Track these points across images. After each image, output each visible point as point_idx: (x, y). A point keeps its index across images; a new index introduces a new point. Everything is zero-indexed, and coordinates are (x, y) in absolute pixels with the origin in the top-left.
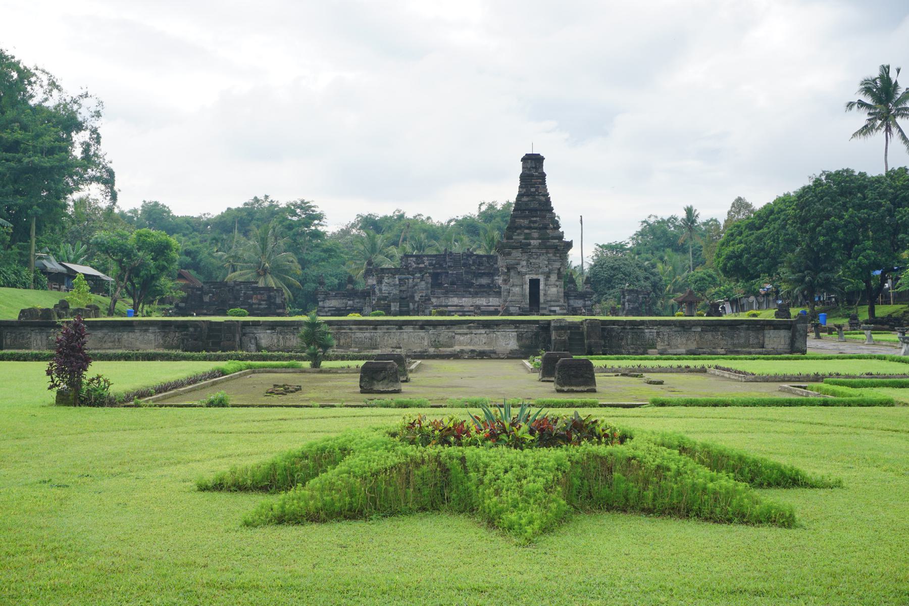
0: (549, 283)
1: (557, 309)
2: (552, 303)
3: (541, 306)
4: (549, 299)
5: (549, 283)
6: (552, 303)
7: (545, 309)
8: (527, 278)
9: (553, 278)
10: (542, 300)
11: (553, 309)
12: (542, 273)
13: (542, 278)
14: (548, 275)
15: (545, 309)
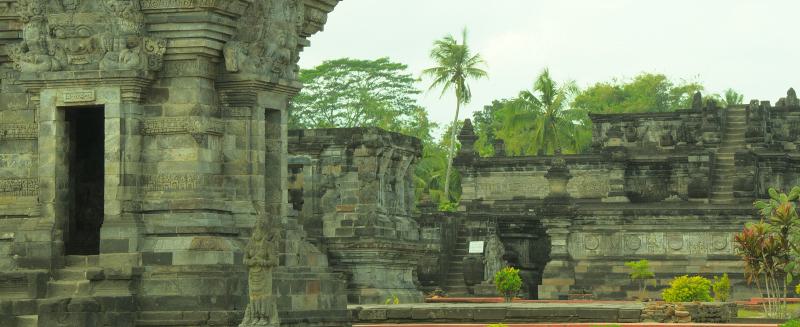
0: (156, 123)
1: (177, 246)
2: (168, 220)
3: (105, 234)
4: (155, 199)
5: (156, 123)
6: (168, 220)
7: (121, 246)
8: (52, 100)
9: (185, 98)
10: (112, 207)
11: (162, 245)
12: (109, 79)
13: (111, 101)
14: (150, 88)
15: (121, 246)
